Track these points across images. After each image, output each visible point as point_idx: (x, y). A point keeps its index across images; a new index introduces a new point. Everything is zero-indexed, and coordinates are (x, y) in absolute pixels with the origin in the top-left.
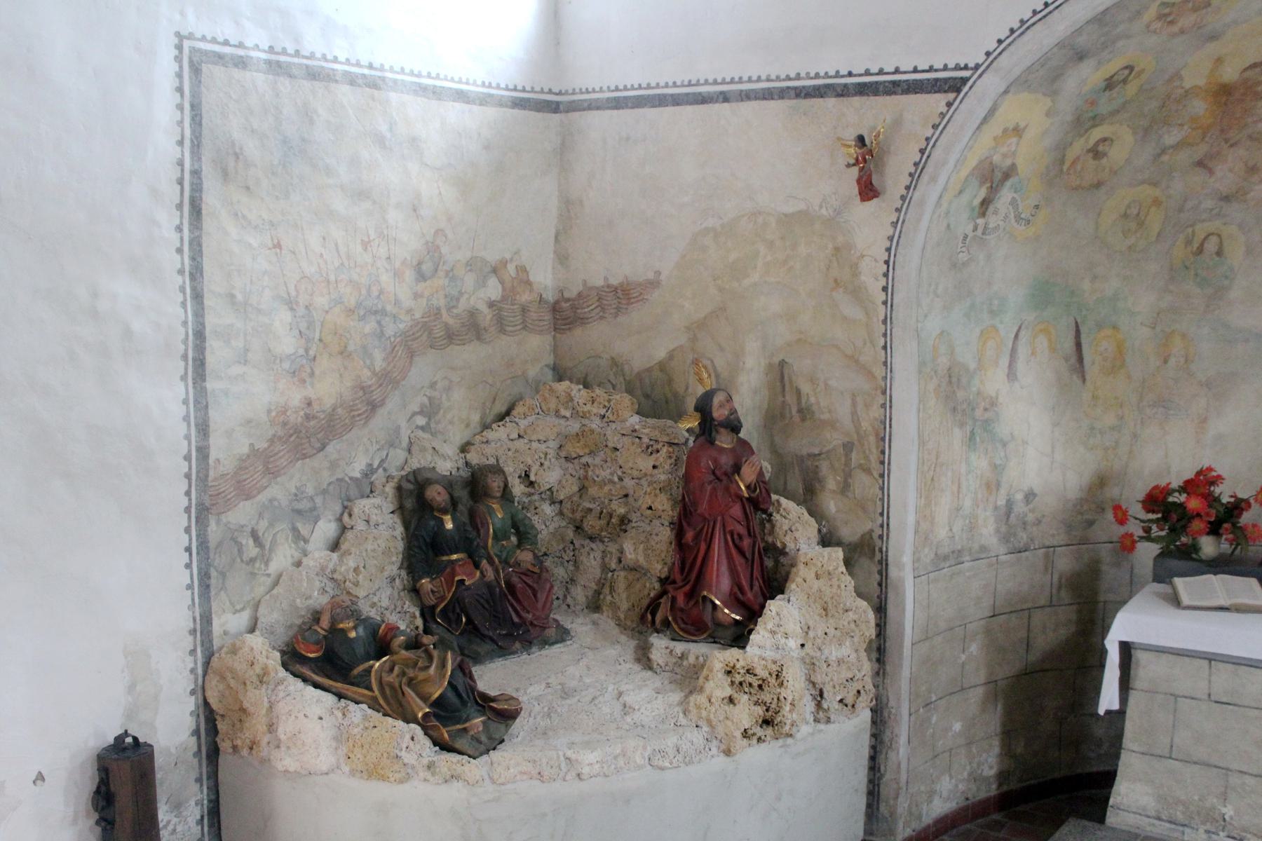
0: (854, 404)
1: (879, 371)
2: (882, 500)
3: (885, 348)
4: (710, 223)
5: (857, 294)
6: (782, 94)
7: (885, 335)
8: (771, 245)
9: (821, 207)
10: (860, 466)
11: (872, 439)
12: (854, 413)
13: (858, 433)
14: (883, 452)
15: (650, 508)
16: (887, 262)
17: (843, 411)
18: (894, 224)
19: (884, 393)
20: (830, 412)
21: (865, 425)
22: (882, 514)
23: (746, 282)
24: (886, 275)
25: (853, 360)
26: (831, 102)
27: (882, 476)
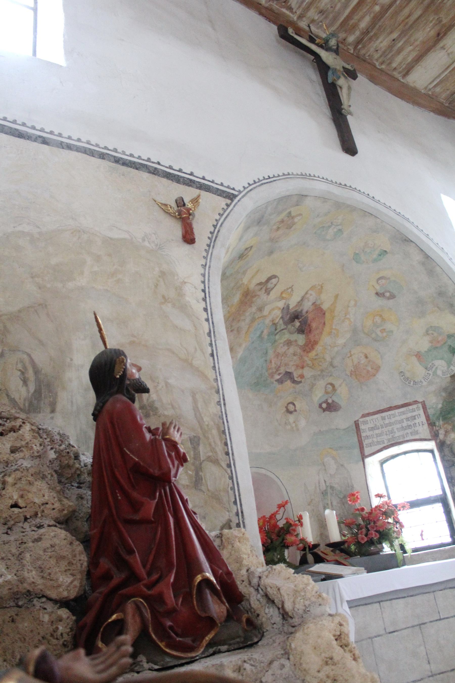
0: (195, 401)
1: (211, 374)
2: (233, 489)
3: (212, 355)
4: (26, 228)
5: (184, 308)
6: (102, 156)
7: (211, 345)
8: (98, 259)
9: (144, 240)
10: (209, 459)
11: (215, 432)
12: (196, 409)
13: (201, 428)
14: (226, 444)
15: (15, 505)
16: (204, 291)
17: (186, 408)
18: (204, 266)
19: (218, 392)
20: (173, 407)
21: (206, 419)
22: (235, 503)
23: (70, 285)
24: (204, 299)
25: (187, 364)
26: (145, 175)
27: (229, 466)
